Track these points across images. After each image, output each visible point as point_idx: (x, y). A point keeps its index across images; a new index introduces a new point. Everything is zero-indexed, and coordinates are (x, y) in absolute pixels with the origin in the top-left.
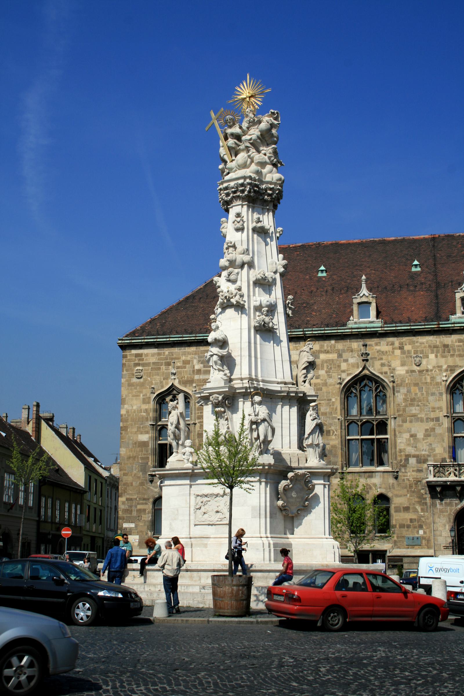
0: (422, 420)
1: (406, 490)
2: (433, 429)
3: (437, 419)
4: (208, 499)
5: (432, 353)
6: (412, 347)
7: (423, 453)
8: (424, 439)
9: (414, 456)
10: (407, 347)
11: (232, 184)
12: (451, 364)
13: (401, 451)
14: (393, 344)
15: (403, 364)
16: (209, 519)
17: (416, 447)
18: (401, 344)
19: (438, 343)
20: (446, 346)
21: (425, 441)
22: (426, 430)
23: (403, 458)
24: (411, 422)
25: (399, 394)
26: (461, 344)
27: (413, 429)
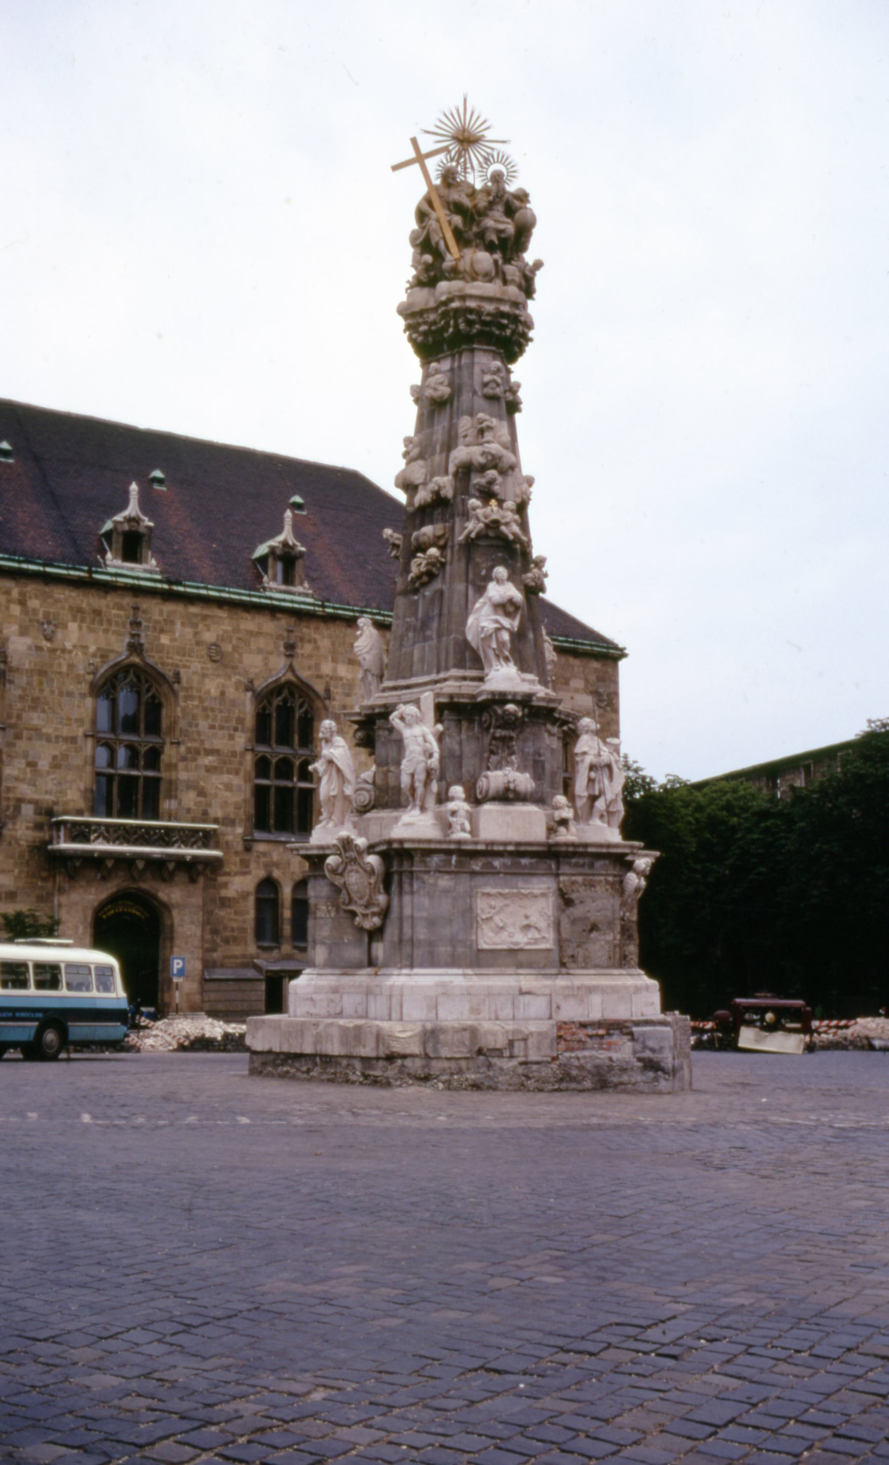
0: (49, 740)
1: (12, 861)
2: (65, 757)
3: (74, 740)
4: (507, 902)
5: (74, 620)
6: (41, 606)
7: (47, 797)
8: (48, 773)
9: (30, 802)
10: (33, 603)
11: (489, 307)
12: (103, 645)
13: (9, 789)
14: (8, 593)
15: (23, 632)
16: (509, 940)
17: (35, 785)
18: (22, 594)
19: (84, 606)
20: (97, 612)
21: (53, 776)
22: (55, 757)
23: (12, 803)
24: (30, 739)
25: (12, 686)
26: (122, 613)
27: (31, 753)
